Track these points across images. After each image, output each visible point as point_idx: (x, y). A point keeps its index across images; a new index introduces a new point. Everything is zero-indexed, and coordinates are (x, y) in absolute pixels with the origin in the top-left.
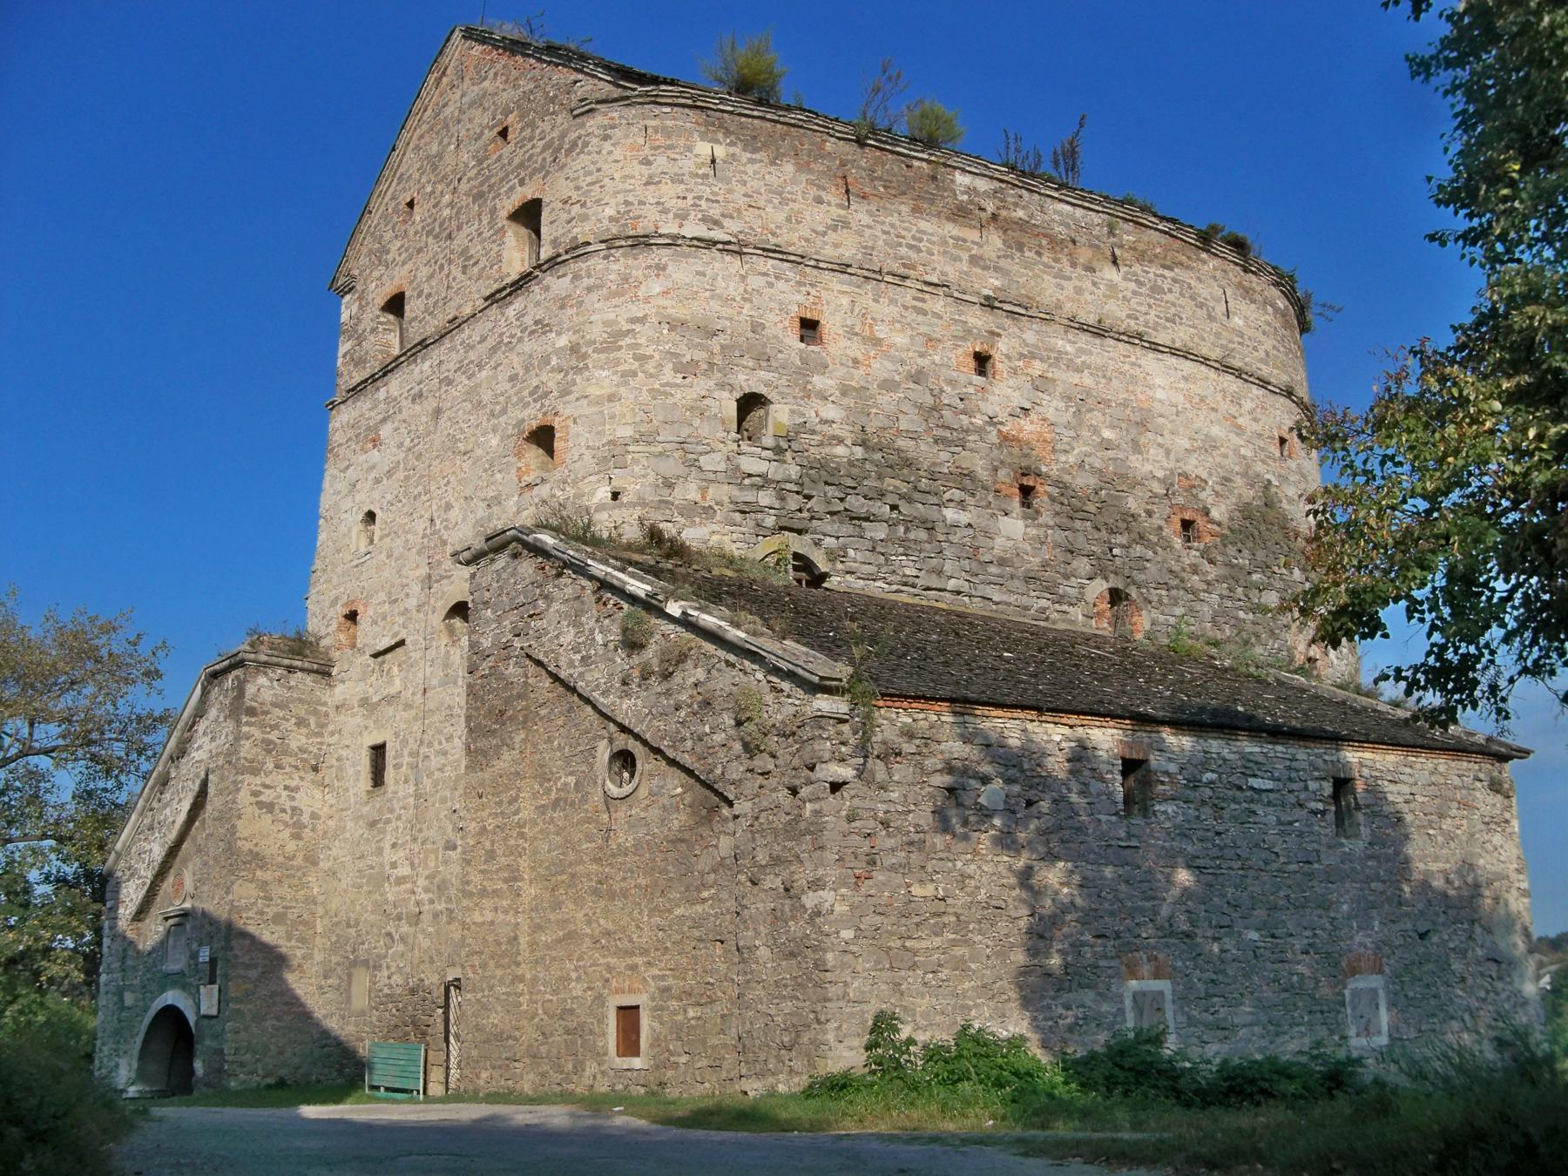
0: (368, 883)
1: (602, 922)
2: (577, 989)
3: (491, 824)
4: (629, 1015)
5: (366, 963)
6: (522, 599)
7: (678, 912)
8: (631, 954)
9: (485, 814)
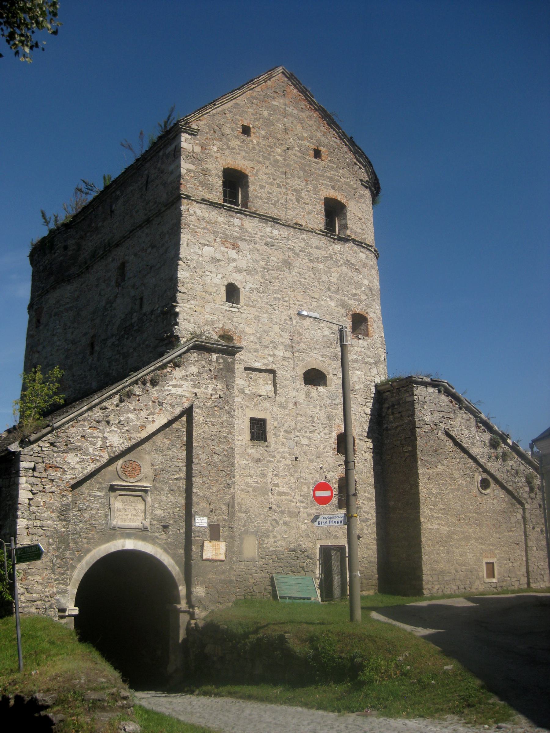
1: (479, 534)
2: (470, 556)
3: (435, 491)
4: (490, 565)
5: (255, 534)
6: (442, 409)
7: (505, 533)
8: (489, 545)
9: (431, 486)
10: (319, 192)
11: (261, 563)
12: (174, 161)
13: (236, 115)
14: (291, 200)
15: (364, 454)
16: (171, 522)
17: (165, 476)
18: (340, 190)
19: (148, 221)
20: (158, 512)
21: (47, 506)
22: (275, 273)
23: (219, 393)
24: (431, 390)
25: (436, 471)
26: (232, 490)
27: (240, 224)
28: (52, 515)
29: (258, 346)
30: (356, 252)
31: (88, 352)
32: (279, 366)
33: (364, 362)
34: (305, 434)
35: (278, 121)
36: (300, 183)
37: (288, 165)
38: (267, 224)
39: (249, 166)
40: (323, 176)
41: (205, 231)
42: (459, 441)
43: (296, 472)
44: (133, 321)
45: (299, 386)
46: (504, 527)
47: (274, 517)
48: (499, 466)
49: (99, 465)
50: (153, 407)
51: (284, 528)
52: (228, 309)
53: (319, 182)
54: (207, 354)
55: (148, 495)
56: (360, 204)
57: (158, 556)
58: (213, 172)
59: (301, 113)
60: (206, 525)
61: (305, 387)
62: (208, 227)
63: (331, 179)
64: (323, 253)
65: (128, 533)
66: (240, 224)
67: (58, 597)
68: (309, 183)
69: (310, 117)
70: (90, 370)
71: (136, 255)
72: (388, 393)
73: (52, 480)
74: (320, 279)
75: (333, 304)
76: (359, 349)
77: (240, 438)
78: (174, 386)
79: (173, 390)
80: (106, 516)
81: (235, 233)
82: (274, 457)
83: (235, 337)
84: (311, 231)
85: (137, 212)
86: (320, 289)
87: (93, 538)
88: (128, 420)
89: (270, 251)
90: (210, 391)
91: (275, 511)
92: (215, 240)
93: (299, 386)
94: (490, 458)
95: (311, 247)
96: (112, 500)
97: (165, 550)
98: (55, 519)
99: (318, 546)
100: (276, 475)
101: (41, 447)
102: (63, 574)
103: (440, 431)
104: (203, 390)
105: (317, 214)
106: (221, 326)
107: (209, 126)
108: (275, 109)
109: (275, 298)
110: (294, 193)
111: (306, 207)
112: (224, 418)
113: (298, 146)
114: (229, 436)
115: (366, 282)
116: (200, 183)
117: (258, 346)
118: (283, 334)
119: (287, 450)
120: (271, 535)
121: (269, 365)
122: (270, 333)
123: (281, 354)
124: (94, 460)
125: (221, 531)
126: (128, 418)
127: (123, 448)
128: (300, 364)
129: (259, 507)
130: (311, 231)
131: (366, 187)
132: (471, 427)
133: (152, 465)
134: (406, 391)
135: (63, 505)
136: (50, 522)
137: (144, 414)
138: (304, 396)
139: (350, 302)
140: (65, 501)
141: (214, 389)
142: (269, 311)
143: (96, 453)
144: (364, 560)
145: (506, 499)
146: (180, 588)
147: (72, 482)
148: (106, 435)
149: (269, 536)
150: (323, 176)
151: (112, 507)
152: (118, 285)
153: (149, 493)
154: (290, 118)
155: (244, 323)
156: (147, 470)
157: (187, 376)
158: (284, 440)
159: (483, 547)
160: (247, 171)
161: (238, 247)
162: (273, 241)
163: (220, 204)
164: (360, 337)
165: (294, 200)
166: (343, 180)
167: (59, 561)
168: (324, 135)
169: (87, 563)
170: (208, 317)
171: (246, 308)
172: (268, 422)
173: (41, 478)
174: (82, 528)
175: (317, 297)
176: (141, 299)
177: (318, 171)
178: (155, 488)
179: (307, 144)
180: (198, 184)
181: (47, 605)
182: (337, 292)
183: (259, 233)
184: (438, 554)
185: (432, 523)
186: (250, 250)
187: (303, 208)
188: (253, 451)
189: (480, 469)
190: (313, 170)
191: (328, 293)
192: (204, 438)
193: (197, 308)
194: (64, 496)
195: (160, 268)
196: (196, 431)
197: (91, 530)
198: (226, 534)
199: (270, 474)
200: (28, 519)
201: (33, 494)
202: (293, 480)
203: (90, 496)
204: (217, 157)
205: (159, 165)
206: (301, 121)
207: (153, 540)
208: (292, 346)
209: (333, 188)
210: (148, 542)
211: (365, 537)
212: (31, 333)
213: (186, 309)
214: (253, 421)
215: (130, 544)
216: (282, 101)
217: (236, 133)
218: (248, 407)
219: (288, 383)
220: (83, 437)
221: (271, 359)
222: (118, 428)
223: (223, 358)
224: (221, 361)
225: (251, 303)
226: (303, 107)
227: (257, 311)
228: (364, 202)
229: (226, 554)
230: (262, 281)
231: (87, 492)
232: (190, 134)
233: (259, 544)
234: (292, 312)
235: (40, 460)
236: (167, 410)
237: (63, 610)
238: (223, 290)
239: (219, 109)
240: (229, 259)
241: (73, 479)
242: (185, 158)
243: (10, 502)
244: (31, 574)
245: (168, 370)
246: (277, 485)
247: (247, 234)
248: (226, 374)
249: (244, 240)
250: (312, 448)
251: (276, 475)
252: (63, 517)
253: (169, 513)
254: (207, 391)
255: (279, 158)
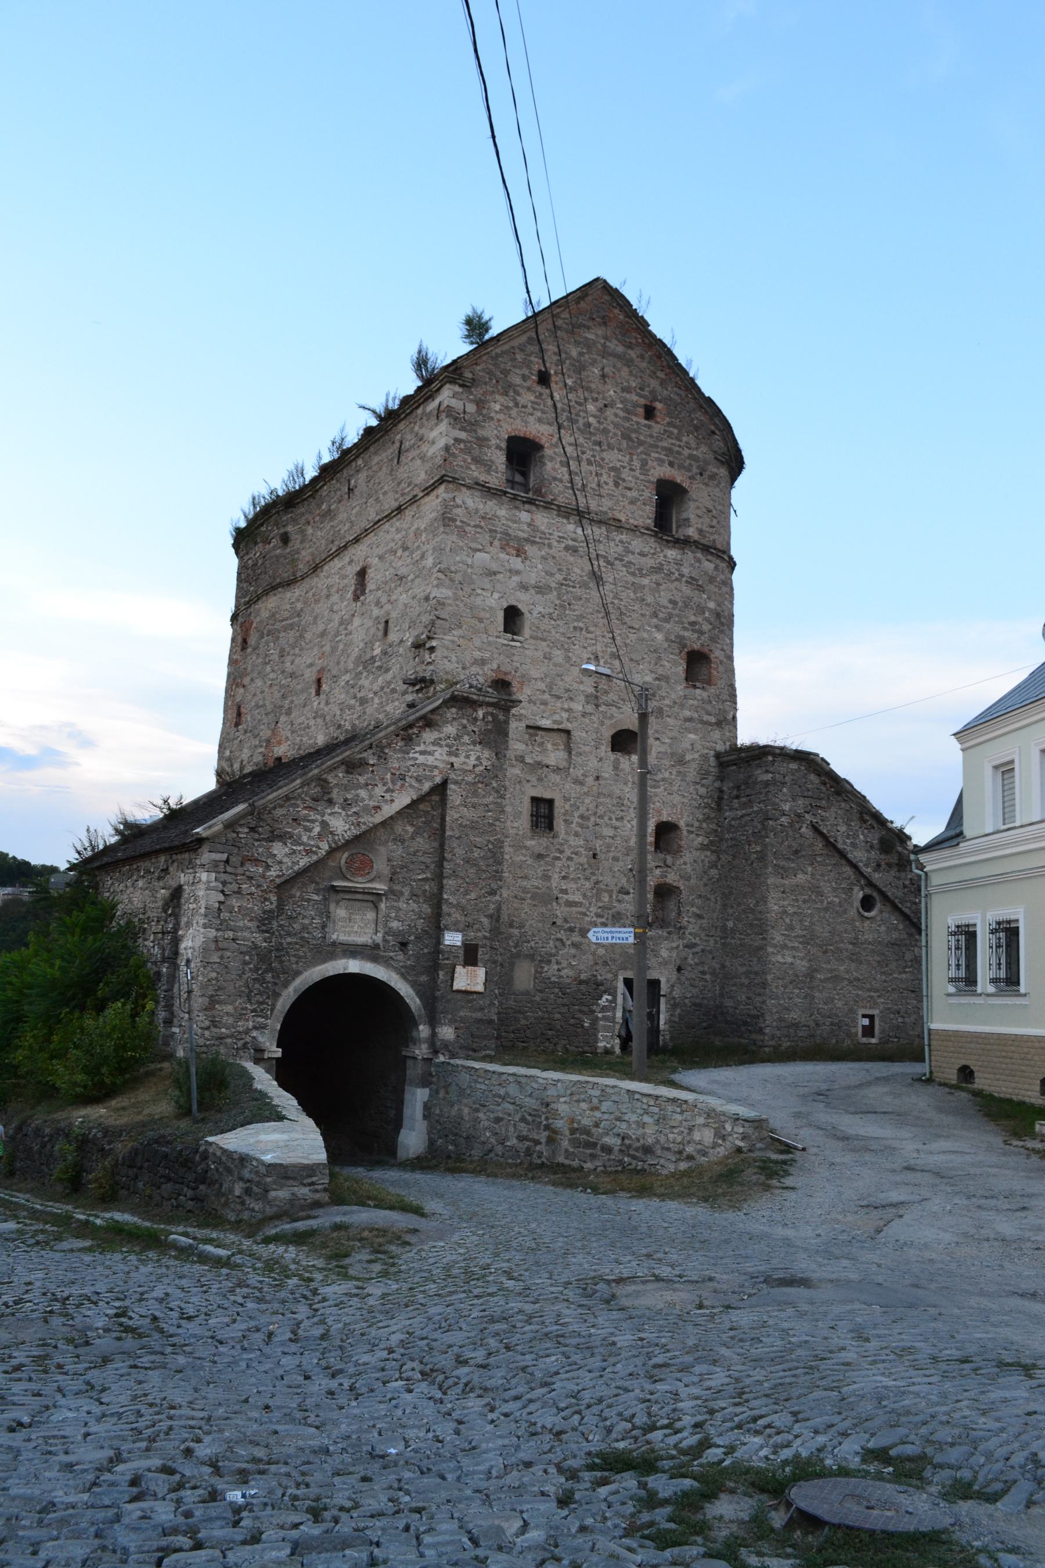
0: (533, 898)
2: (840, 1004)
5: (531, 957)
6: (810, 793)
7: (895, 975)
8: (869, 990)
9: (786, 903)
10: (649, 471)
11: (537, 998)
12: (437, 425)
13: (530, 356)
14: (606, 483)
15: (694, 852)
16: (412, 938)
17: (407, 875)
18: (681, 467)
19: (400, 510)
20: (395, 925)
21: (243, 912)
22: (578, 591)
23: (485, 763)
24: (794, 766)
25: (794, 881)
26: (497, 898)
27: (529, 520)
28: (250, 924)
29: (546, 696)
30: (699, 561)
31: (313, 691)
32: (575, 724)
33: (702, 722)
34: (609, 822)
35: (594, 363)
36: (620, 457)
37: (605, 431)
38: (568, 519)
39: (546, 433)
40: (657, 447)
41: (478, 530)
42: (832, 840)
43: (593, 874)
44: (375, 653)
45: (603, 754)
46: (893, 965)
47: (559, 936)
48: (891, 879)
49: (315, 858)
50: (393, 782)
51: (573, 951)
52: (506, 642)
53: (650, 455)
54: (470, 710)
55: (381, 901)
56: (709, 489)
57: (392, 984)
58: (493, 442)
59: (630, 352)
60: (459, 944)
61: (612, 756)
62: (483, 524)
63: (669, 451)
64: (650, 562)
65: (353, 951)
66: (529, 520)
67: (254, 1034)
68: (635, 457)
69: (642, 357)
70: (314, 718)
71: (381, 558)
72: (734, 767)
73: (252, 878)
74: (643, 600)
75: (660, 637)
76: (695, 702)
77: (516, 825)
78: (422, 753)
79: (421, 759)
80: (324, 926)
81: (521, 534)
82: (561, 852)
83: (515, 683)
84: (634, 530)
85: (385, 493)
86: (642, 615)
87: (305, 957)
88: (357, 799)
89: (572, 559)
90: (472, 761)
91: (561, 927)
92: (491, 544)
93: (603, 754)
94: (879, 865)
95: (633, 553)
96: (332, 907)
97: (403, 976)
98: (253, 930)
99: (621, 978)
100: (564, 878)
101: (238, 833)
102: (262, 1003)
103: (805, 826)
104: (462, 759)
105: (644, 504)
106: (495, 666)
107: (490, 373)
108: (589, 345)
109: (575, 628)
110: (612, 474)
111: (629, 494)
112: (491, 799)
113: (622, 402)
114: (497, 823)
115: (712, 605)
116: (472, 459)
117: (546, 696)
118: (585, 679)
119: (582, 843)
120: (553, 960)
121: (562, 723)
122: (566, 678)
123: (581, 708)
124: (308, 852)
125: (480, 953)
126: (357, 795)
127: (348, 836)
128: (608, 722)
129: (539, 921)
130: (634, 530)
131: (723, 463)
132: (852, 820)
133: (389, 860)
134: (759, 766)
135: (264, 912)
136: (246, 934)
137: (379, 791)
138: (611, 768)
139: (686, 634)
140: (268, 906)
141: (478, 758)
142: (566, 646)
143: (312, 843)
144: (687, 1001)
145: (901, 927)
146: (421, 1027)
147: (278, 881)
148: (326, 818)
149: (550, 961)
150: (657, 447)
151: (332, 915)
152: (356, 598)
153: (384, 898)
154: (611, 358)
155: (528, 662)
156: (381, 866)
157: (440, 739)
158: (579, 829)
159: (860, 993)
160: (543, 441)
161: (525, 553)
162: (577, 544)
163: (500, 490)
164: (698, 684)
165: (611, 484)
166: (686, 452)
167: (257, 986)
168: (661, 384)
169: (295, 991)
170: (477, 654)
171: (532, 641)
172: (557, 804)
173: (236, 875)
174: (289, 943)
175: (637, 626)
176: (387, 622)
177: (648, 440)
178: (391, 891)
179: (635, 398)
180: (469, 461)
181: (240, 1044)
182: (667, 620)
183: (555, 533)
184: (791, 999)
185: (785, 957)
186: (543, 557)
187: (623, 496)
188: (533, 843)
189: (862, 882)
190: (642, 438)
191: (655, 620)
192: (461, 825)
193: (461, 641)
194: (266, 899)
195: (412, 581)
196: (451, 816)
197: (302, 946)
198: (487, 957)
199: (556, 876)
200: (217, 930)
201: (224, 895)
202: (588, 885)
203: (303, 899)
204: (499, 420)
205: (416, 428)
206: (629, 363)
207: (387, 962)
208: (597, 697)
209: (671, 464)
210: (379, 963)
211: (689, 969)
212: (235, 657)
213: (446, 642)
214: (536, 801)
215: (354, 966)
216: (600, 332)
217: (528, 383)
218: (528, 781)
219: (587, 749)
220: (295, 820)
221: (565, 715)
222: (343, 809)
223: (492, 714)
224: (490, 718)
225: (540, 635)
226: (634, 341)
227: (548, 646)
228: (717, 486)
229: (485, 984)
230: (557, 602)
231: (298, 894)
232: (460, 386)
233: (536, 971)
234: (599, 648)
235: (236, 851)
236: (411, 786)
237: (260, 1051)
238: (500, 616)
239: (506, 347)
240: (510, 571)
241: (278, 876)
242: (452, 421)
243: (194, 906)
244: (219, 1002)
245: (415, 731)
246: (565, 892)
247: (539, 534)
248: (495, 737)
249: (533, 543)
250: (619, 841)
251: (564, 878)
252: (264, 928)
253: (409, 925)
254: (467, 760)
255: (591, 419)
